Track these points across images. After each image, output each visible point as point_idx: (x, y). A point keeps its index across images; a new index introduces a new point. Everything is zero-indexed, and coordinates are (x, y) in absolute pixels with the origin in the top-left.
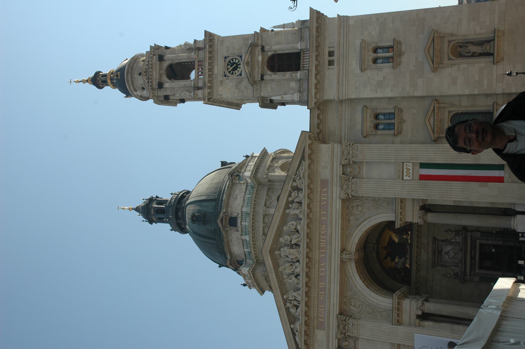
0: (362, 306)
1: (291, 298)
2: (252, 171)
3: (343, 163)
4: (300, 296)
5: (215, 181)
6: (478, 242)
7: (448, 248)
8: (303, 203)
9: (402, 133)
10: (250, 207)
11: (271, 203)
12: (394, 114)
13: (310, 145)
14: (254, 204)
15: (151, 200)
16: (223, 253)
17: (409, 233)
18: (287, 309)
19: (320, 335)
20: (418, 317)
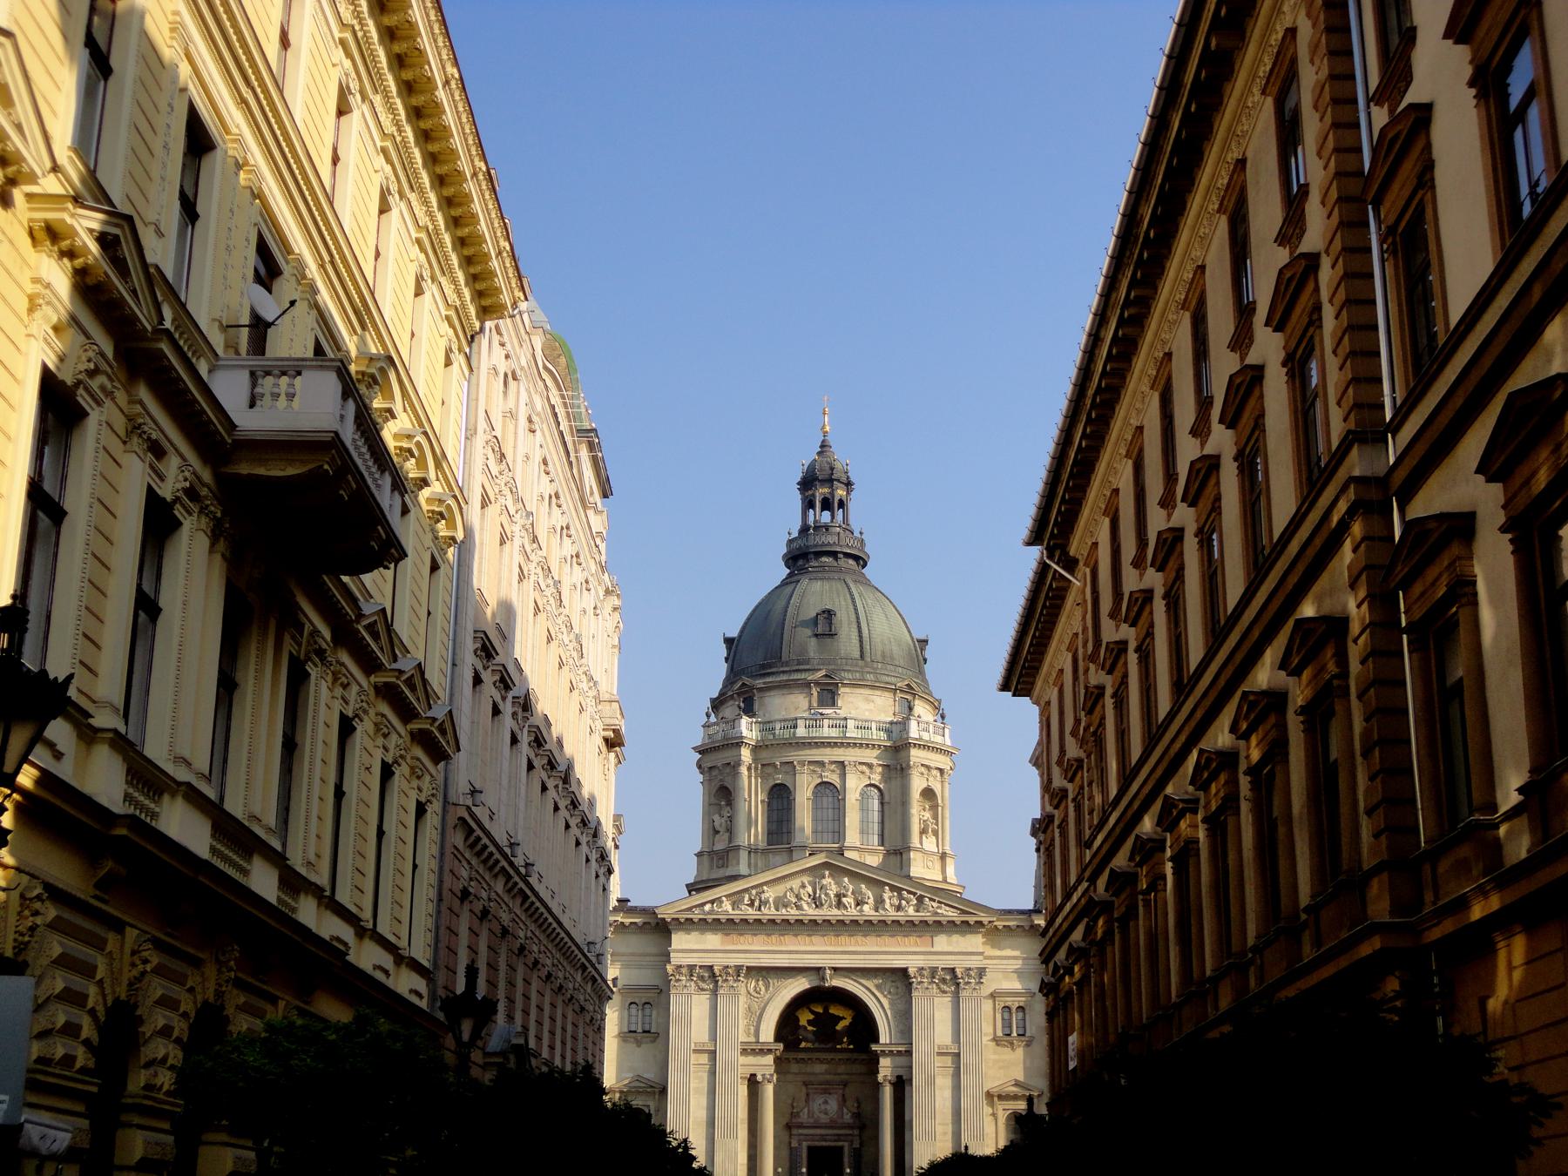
0: (756, 995)
1: (763, 896)
2: (921, 739)
3: (957, 970)
4: (769, 912)
5: (895, 649)
6: (846, 1144)
7: (833, 1105)
8: (899, 913)
9: (999, 1048)
10: (854, 735)
11: (863, 773)
12: (1023, 1035)
13: (980, 923)
14: (861, 744)
15: (848, 484)
16: (764, 670)
17: (851, 1047)
18: (746, 890)
19: (713, 940)
20: (753, 1076)
